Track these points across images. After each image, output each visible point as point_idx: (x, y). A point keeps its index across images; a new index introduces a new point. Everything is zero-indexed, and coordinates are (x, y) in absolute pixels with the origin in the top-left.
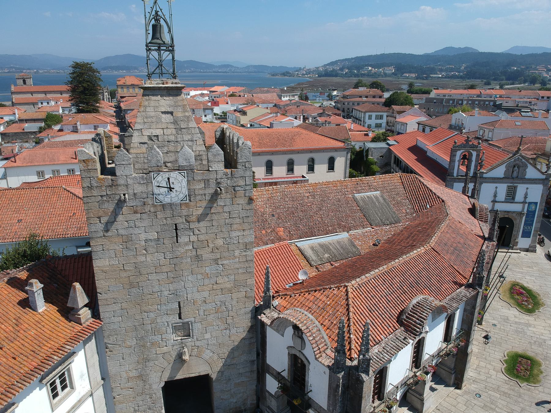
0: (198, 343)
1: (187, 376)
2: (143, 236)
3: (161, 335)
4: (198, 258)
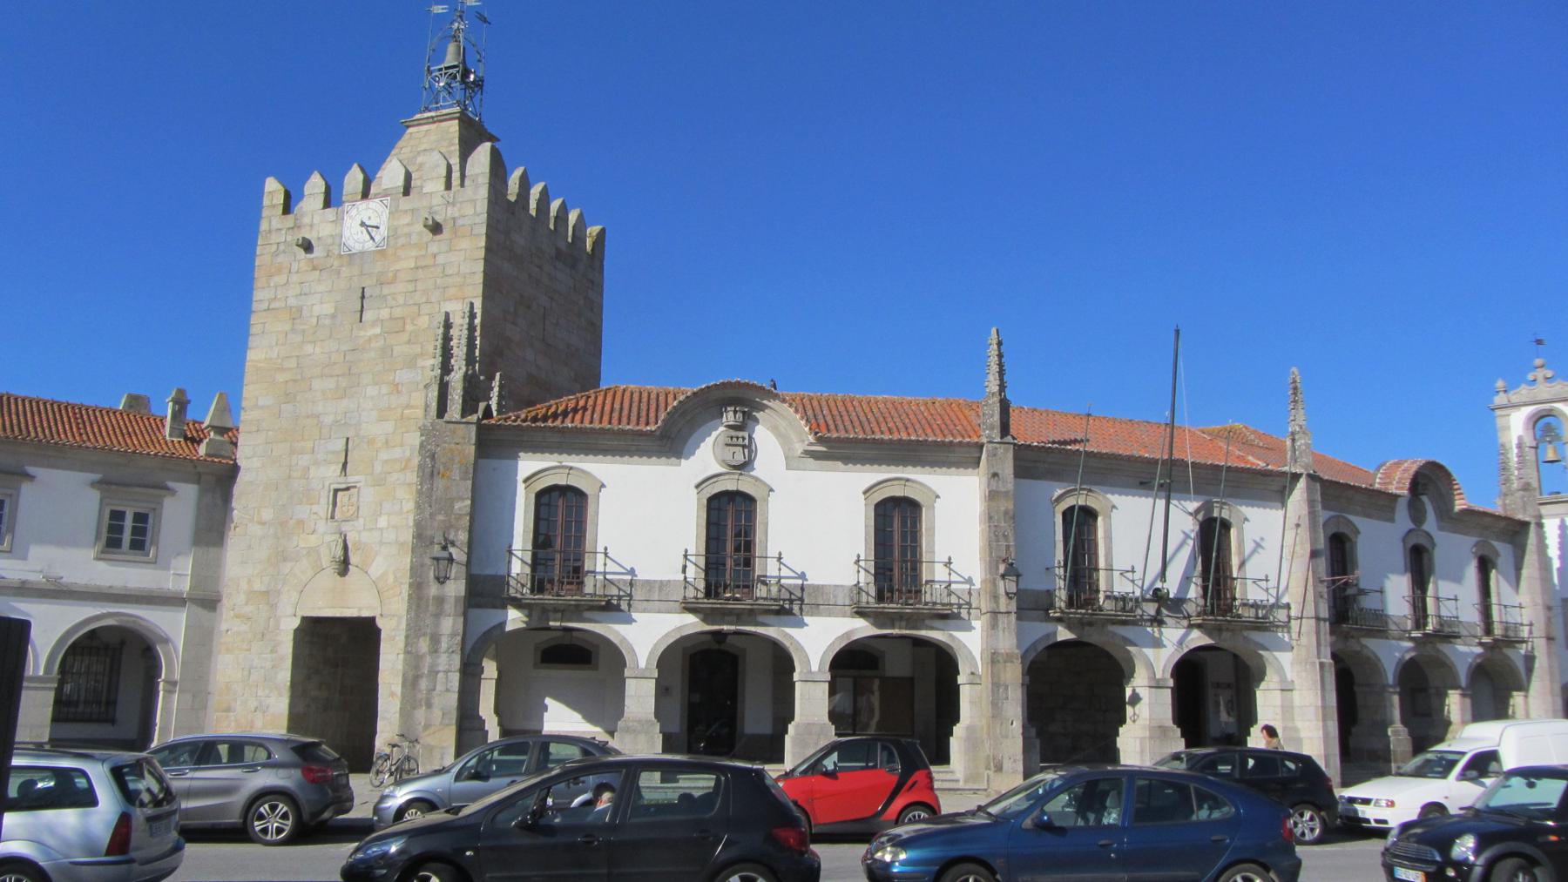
2: (317, 310)
4: (386, 351)
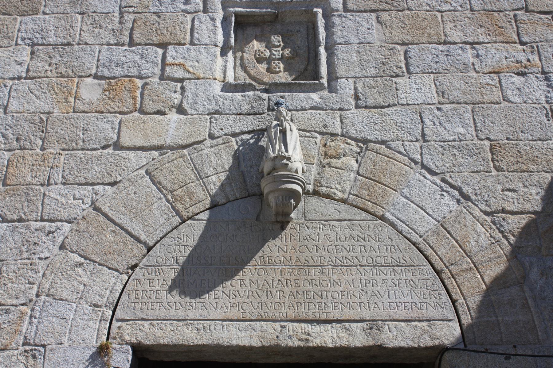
0: (359, 121)
1: (292, 336)
3: (163, 46)
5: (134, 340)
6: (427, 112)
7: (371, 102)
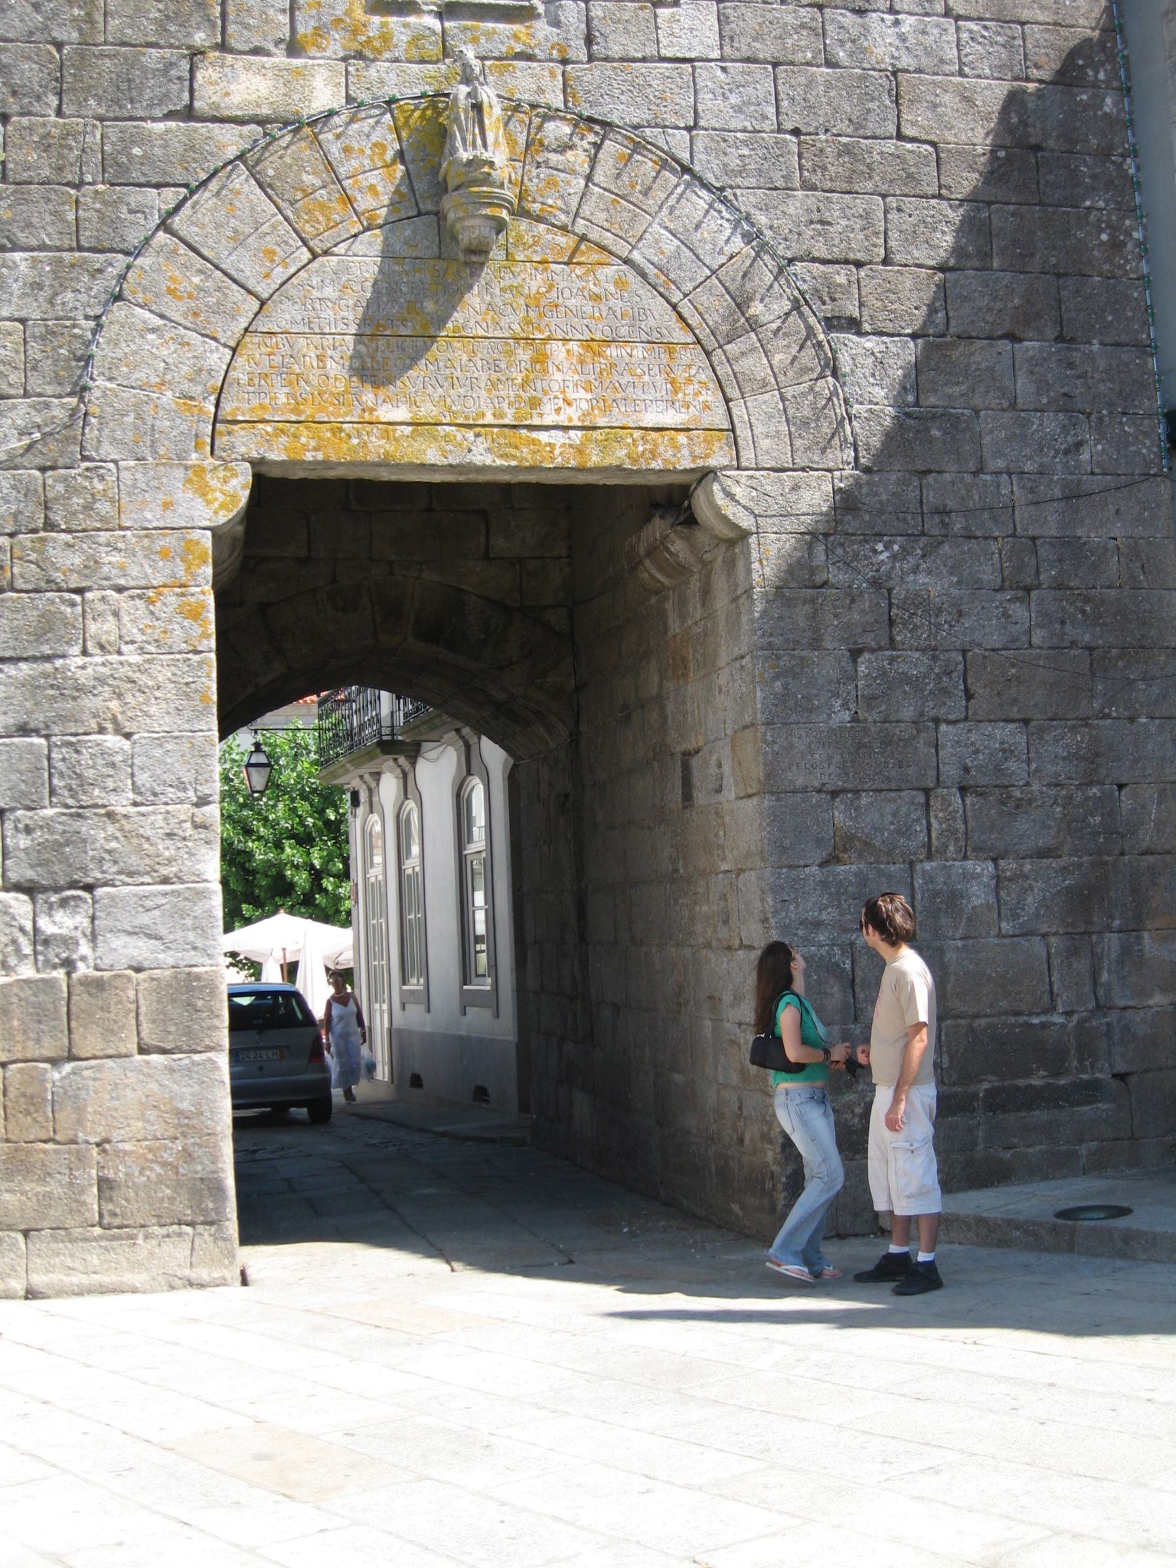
5: (255, 455)
6: (705, 74)
7: (616, 50)
